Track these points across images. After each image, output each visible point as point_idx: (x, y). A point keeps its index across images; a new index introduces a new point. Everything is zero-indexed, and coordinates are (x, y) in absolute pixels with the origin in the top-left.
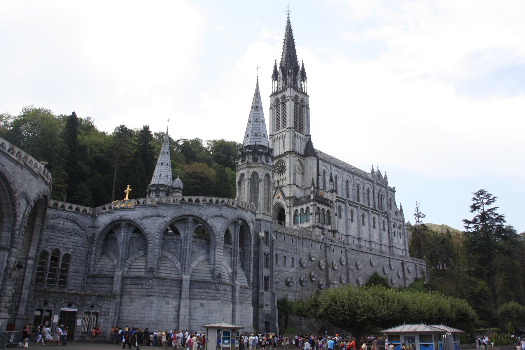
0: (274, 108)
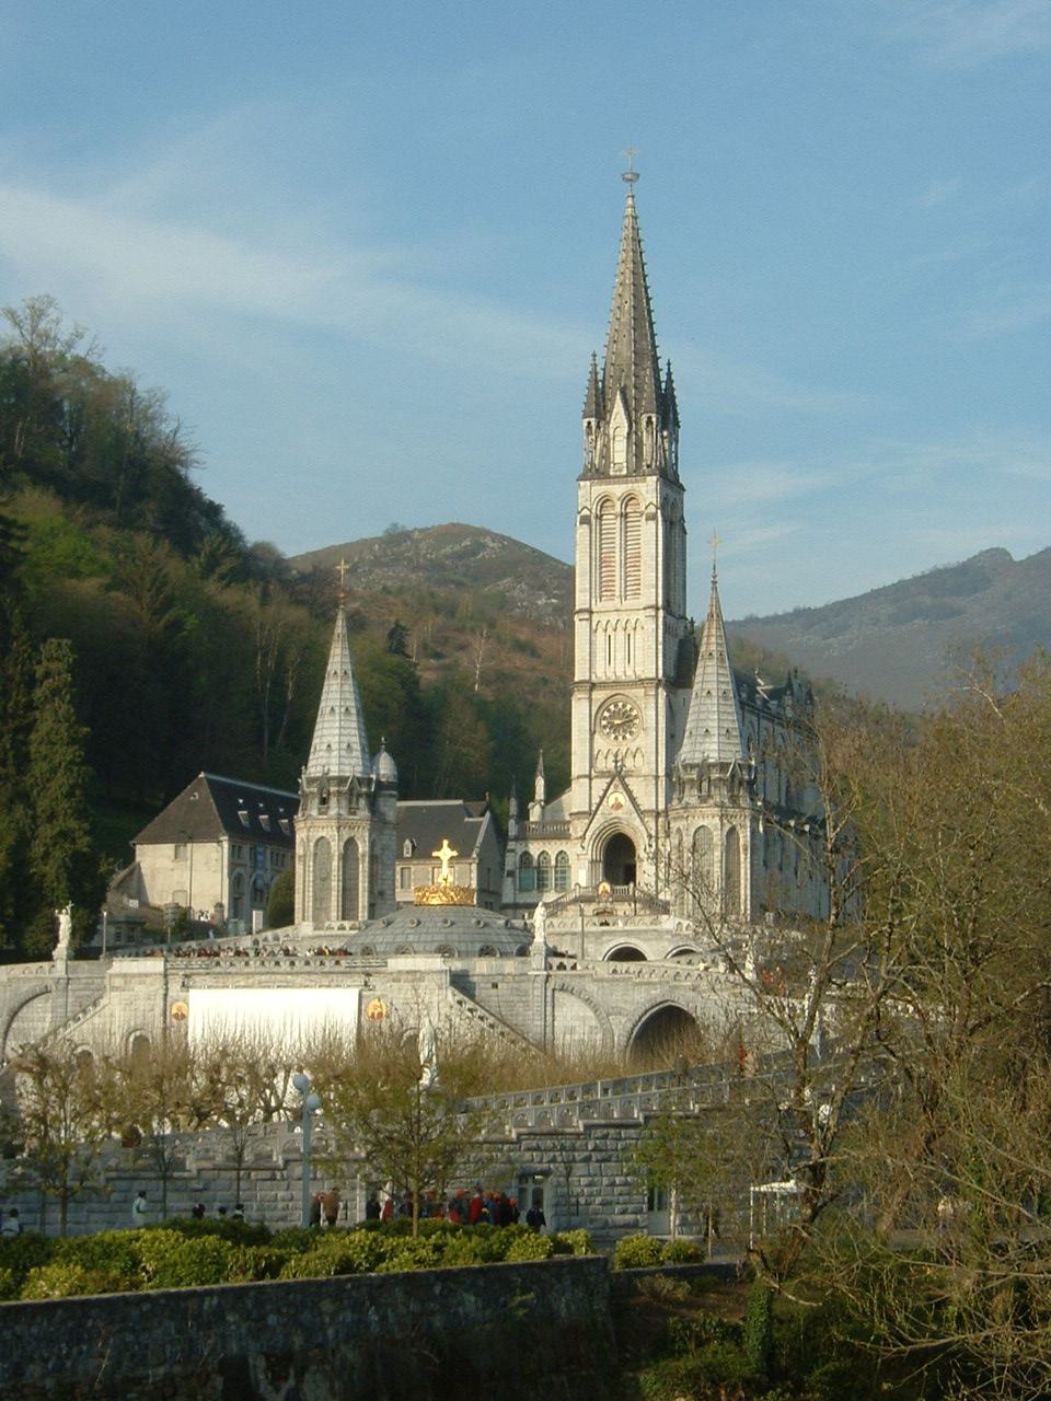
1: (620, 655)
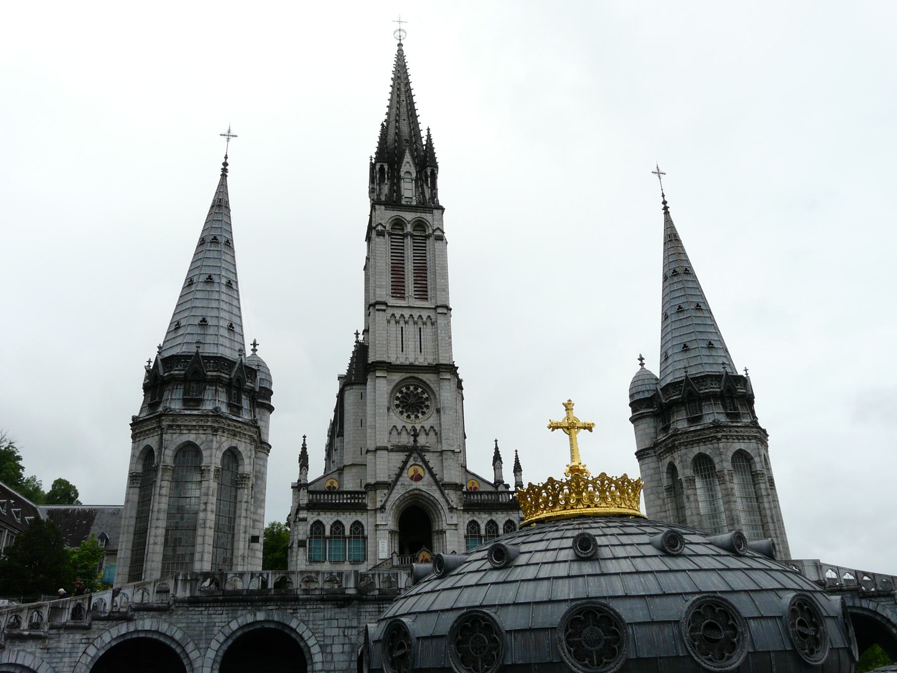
0: (387, 236)
1: (411, 344)
